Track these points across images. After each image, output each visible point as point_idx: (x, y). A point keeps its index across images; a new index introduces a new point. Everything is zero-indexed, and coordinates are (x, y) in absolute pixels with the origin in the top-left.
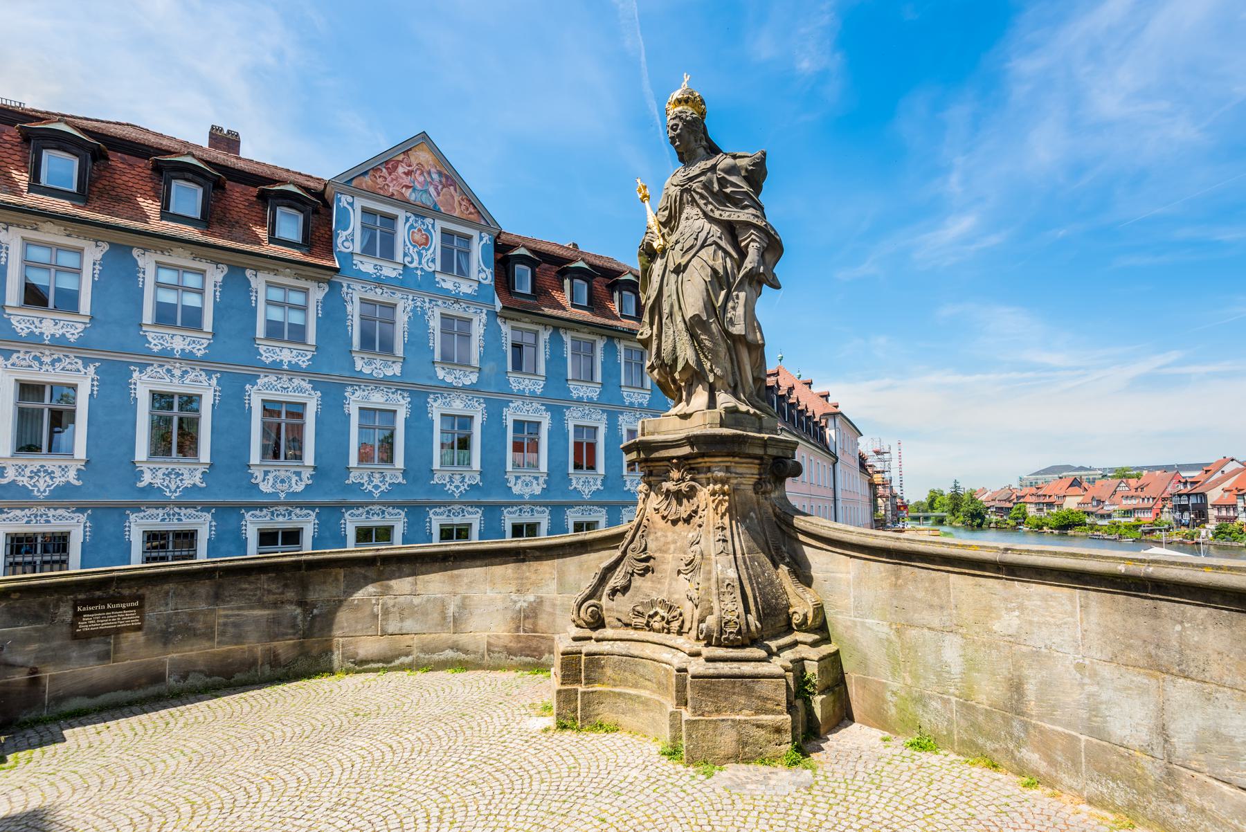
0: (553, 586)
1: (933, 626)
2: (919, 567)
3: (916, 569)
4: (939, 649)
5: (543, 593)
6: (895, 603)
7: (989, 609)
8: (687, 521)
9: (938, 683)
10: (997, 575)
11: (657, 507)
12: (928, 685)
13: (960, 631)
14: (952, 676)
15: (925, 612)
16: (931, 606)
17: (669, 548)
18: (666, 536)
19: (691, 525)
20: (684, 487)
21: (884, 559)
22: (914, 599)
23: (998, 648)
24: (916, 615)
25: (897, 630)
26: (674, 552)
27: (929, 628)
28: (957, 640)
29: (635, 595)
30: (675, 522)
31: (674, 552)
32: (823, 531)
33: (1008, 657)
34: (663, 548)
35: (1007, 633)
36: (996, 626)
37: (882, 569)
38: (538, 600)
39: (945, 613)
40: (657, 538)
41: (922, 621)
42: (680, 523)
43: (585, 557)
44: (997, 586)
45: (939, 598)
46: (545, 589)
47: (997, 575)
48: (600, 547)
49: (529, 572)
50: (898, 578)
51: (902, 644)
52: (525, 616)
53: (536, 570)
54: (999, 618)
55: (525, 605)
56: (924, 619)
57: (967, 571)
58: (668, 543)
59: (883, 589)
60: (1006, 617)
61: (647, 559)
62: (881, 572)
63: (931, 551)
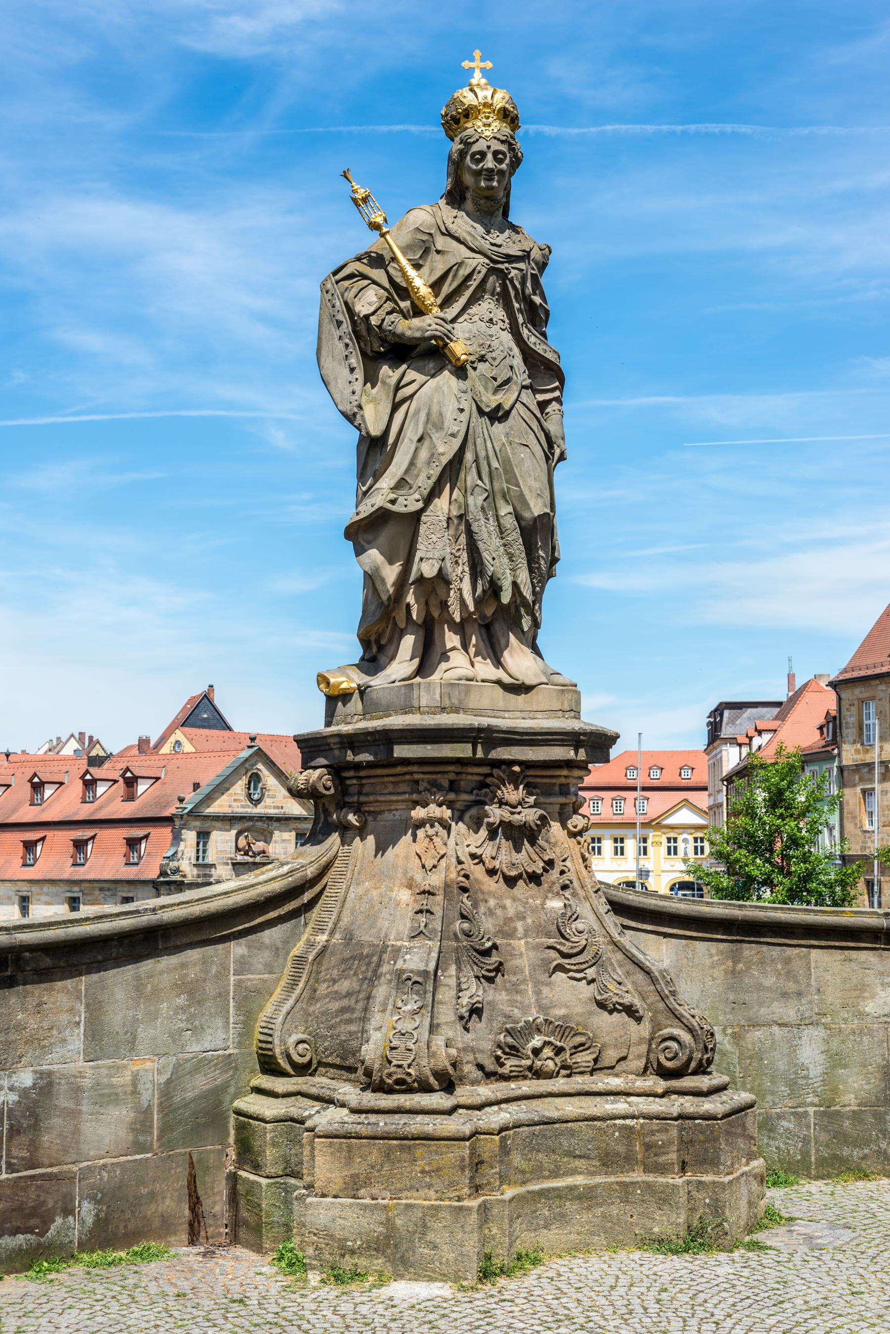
0: (77, 1041)
1: (786, 1020)
2: (768, 944)
3: (765, 948)
4: (793, 1049)
5: (52, 1063)
6: (732, 998)
7: (862, 989)
8: (534, 879)
9: (792, 1095)
10: (874, 946)
11: (479, 851)
12: (777, 1100)
13: (823, 1021)
14: (810, 1081)
15: (776, 1004)
16: (785, 995)
17: (515, 929)
18: (504, 907)
19: (545, 886)
20: (529, 815)
21: (719, 937)
22: (760, 987)
23: (870, 1032)
24: (762, 1010)
25: (734, 1035)
26: (526, 936)
27: (780, 1025)
28: (818, 1033)
29: (490, 1020)
30: (511, 882)
31: (526, 936)
32: (630, 897)
33: (883, 1041)
34: (506, 928)
35: (882, 1013)
36: (870, 1007)
37: (714, 951)
38: (41, 1083)
39: (804, 1001)
40: (490, 910)
41: (770, 1017)
42: (521, 883)
43: (147, 966)
44: (872, 959)
45: (797, 982)
46: (58, 1053)
47: (874, 946)
48: (185, 940)
49: (24, 1010)
50: (736, 962)
51: (741, 1054)
52: (11, 1127)
53: (39, 1005)
54: (873, 997)
55: (13, 1097)
56: (774, 1013)
57: (837, 944)
58: (511, 919)
59: (714, 979)
60: (882, 994)
61: (486, 953)
62: (711, 956)
63: (798, 921)
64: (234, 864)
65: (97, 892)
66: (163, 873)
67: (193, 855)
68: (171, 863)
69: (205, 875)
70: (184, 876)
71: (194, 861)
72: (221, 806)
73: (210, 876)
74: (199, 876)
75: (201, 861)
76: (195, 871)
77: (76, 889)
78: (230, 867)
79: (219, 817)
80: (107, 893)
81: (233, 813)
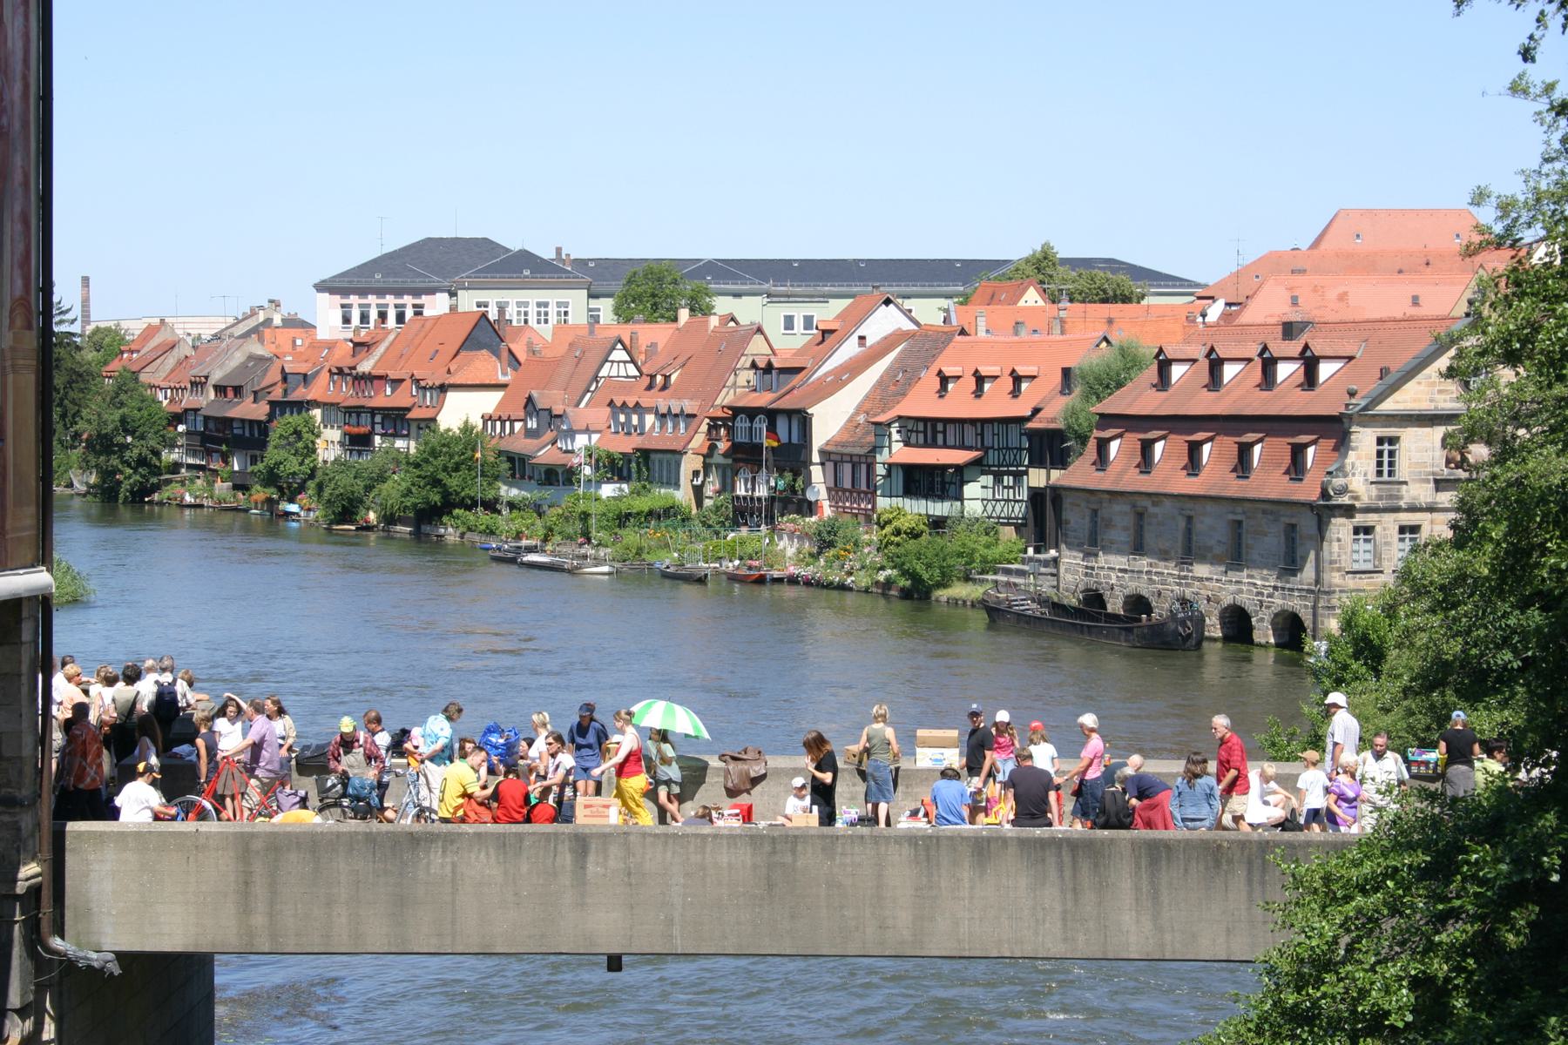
64: (1436, 481)
65: (1260, 516)
66: (1325, 495)
67: (1372, 467)
68: (1334, 480)
69: (1391, 497)
70: (1356, 498)
71: (1372, 477)
72: (1409, 398)
73: (1400, 498)
74: (1380, 498)
75: (1385, 477)
76: (1374, 490)
77: (1239, 510)
78: (1432, 485)
79: (1411, 416)
80: (1270, 517)
81: (1436, 409)
